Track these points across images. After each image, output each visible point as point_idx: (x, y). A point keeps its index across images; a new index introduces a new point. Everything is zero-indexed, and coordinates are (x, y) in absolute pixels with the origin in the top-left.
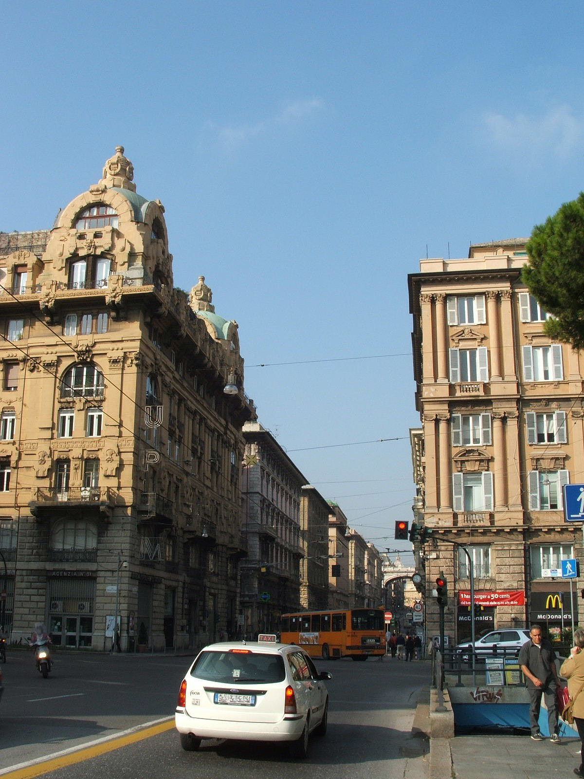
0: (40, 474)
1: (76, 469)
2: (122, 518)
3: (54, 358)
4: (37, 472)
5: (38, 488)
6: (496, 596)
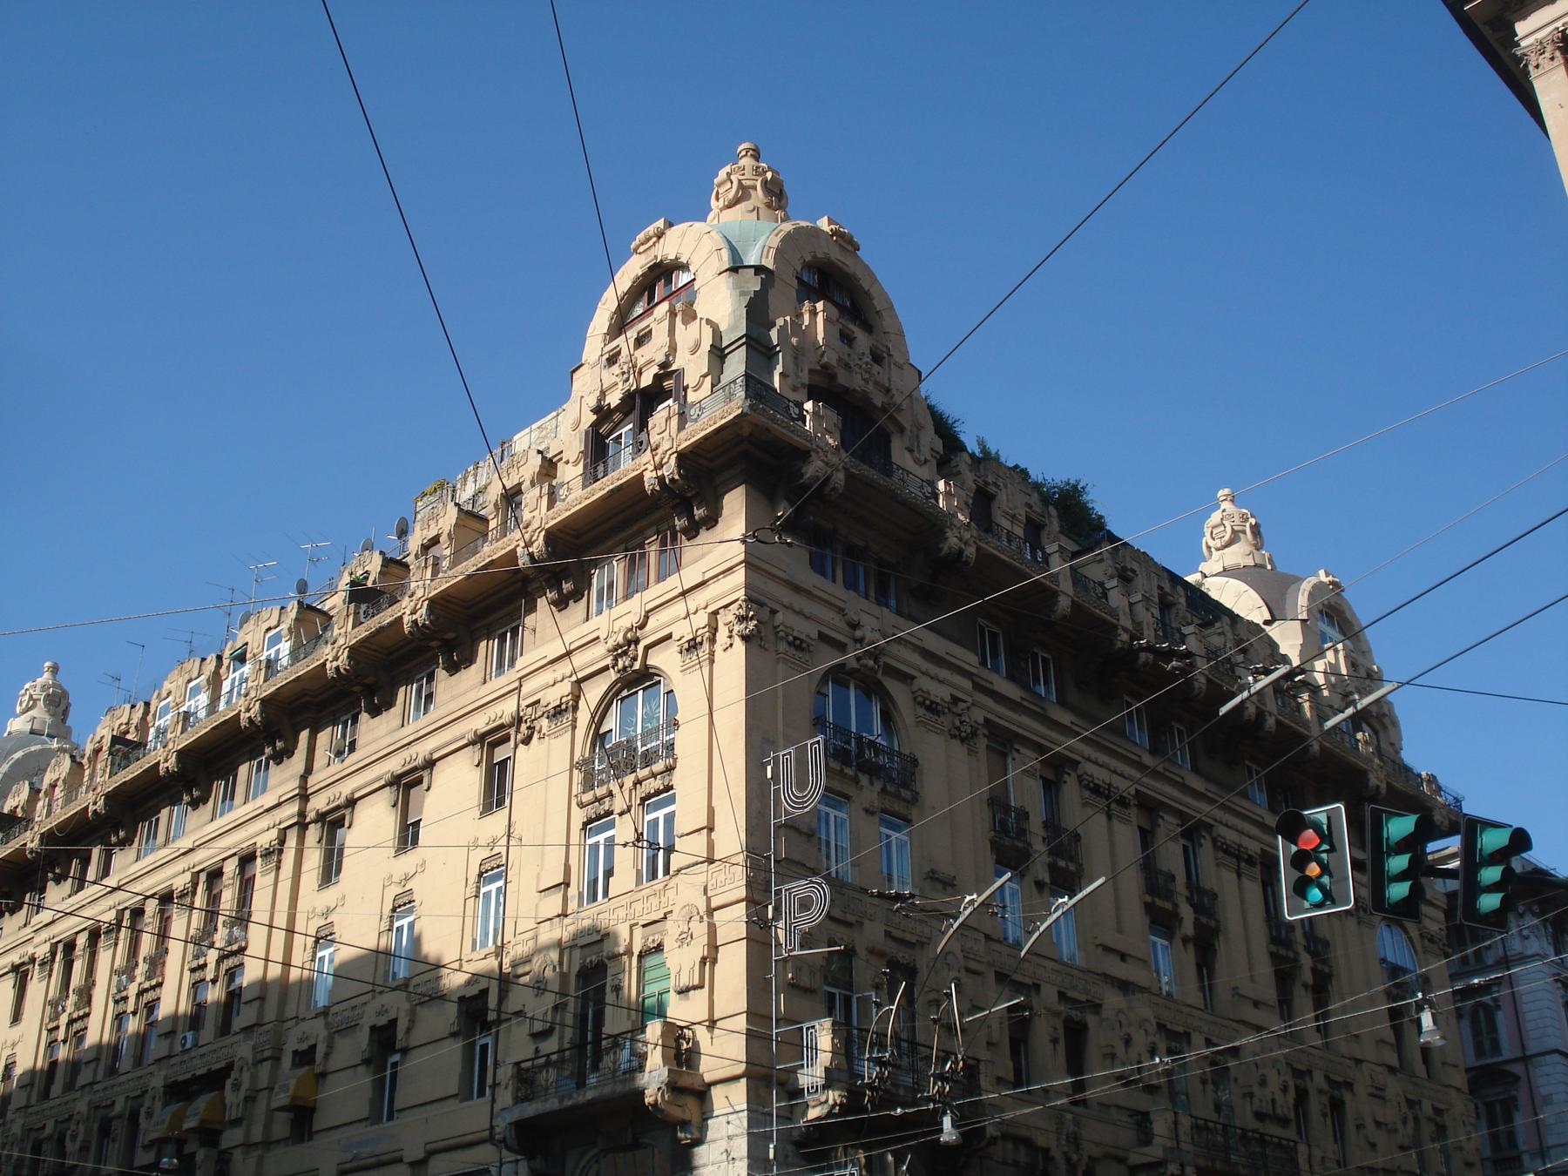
0: (538, 1027)
2: (723, 1119)
3: (566, 688)
5: (517, 1064)
6: (805, 905)
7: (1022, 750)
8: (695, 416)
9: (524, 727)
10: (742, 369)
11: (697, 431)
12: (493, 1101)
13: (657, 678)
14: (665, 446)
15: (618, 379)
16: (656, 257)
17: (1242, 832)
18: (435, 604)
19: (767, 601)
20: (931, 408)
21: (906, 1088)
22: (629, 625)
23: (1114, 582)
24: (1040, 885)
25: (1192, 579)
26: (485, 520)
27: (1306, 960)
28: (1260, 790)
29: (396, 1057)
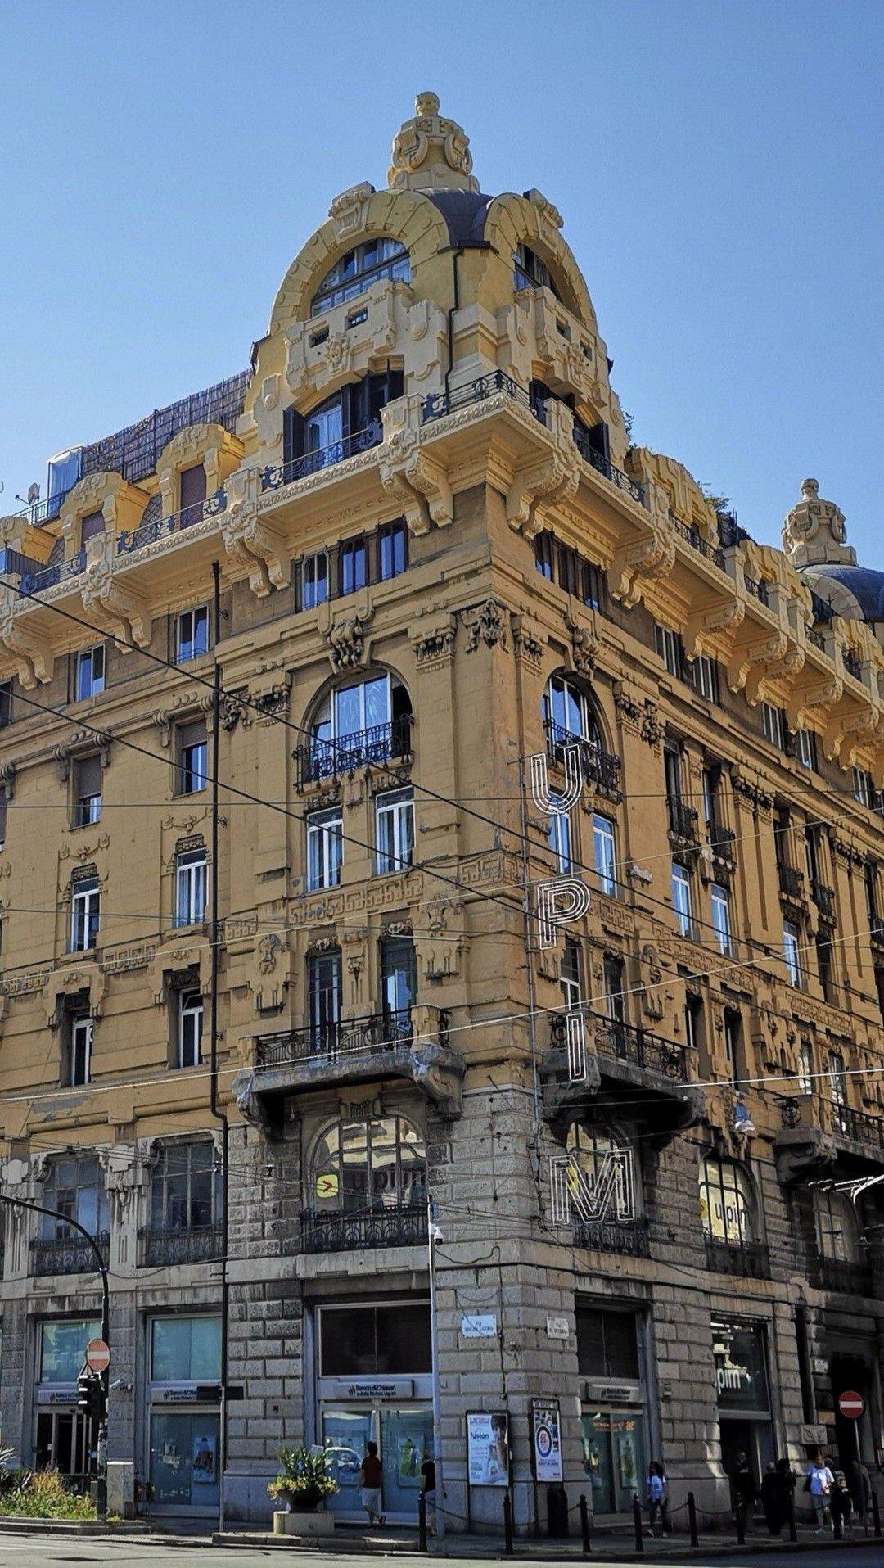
0: (267, 1002)
1: (356, 972)
2: (489, 1097)
4: (259, 998)
5: (257, 1037)
7: (691, 752)
19: (511, 607)
24: (705, 881)
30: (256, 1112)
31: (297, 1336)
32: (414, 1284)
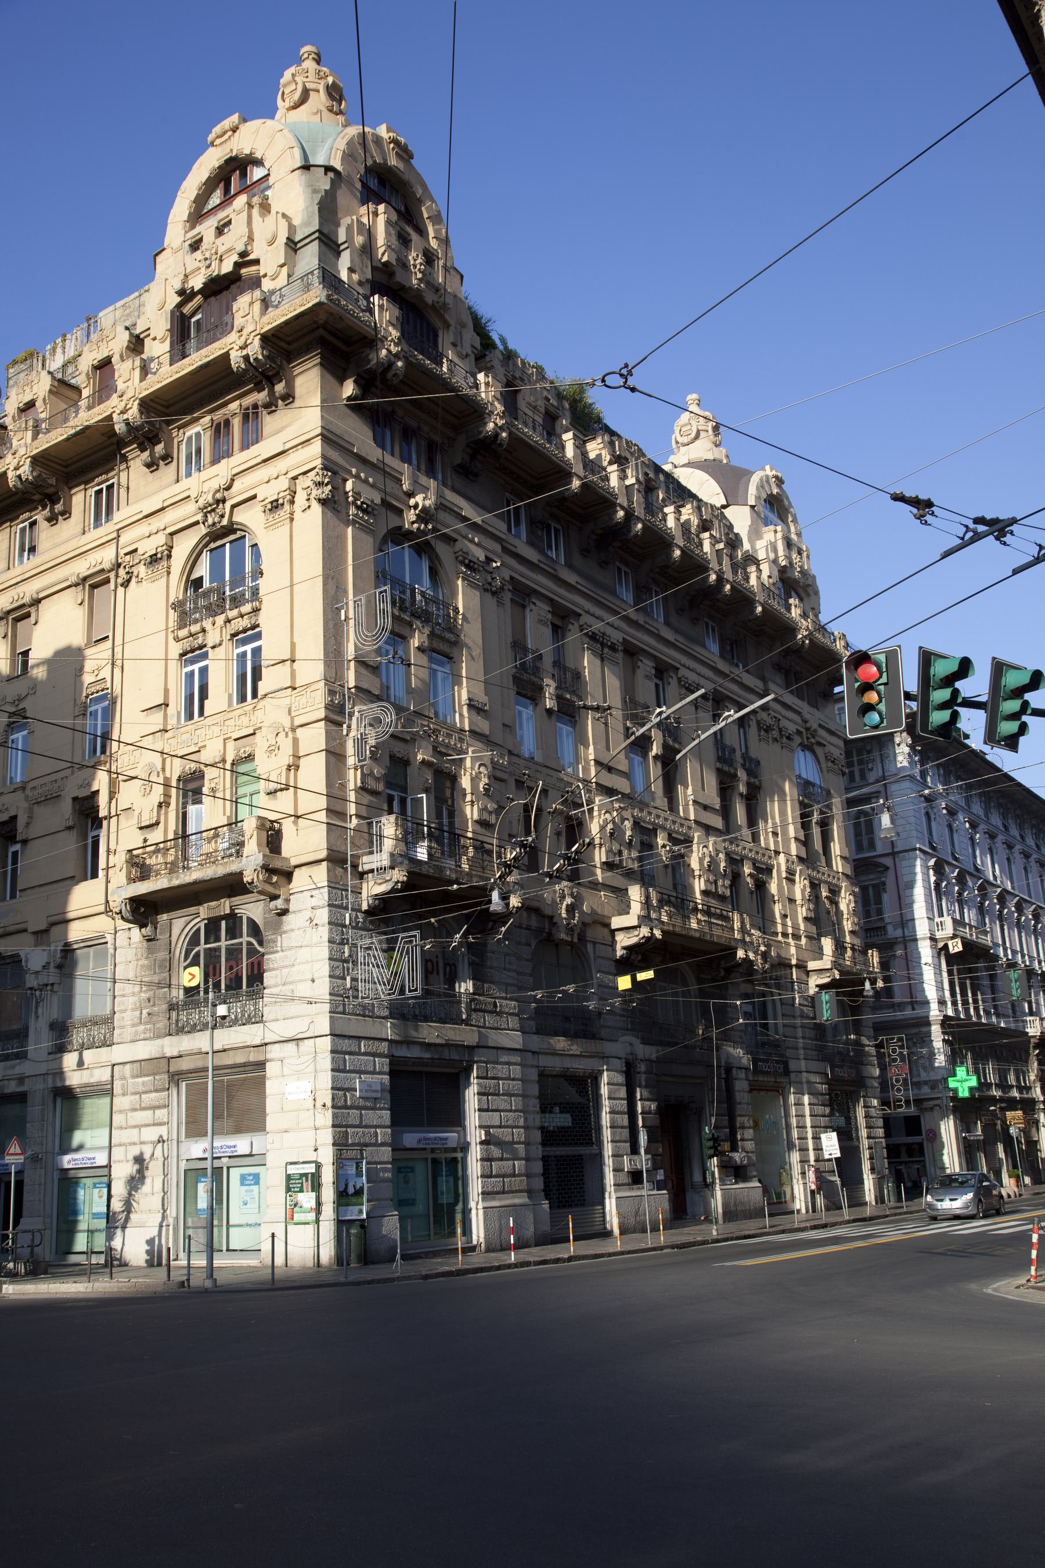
2: (309, 894)
3: (161, 539)
5: (130, 851)
7: (538, 603)
8: (276, 303)
9: (122, 572)
10: (315, 263)
11: (277, 317)
12: (108, 882)
13: (243, 533)
14: (249, 328)
15: (200, 265)
16: (232, 150)
17: (699, 674)
18: (37, 461)
20: (470, 308)
21: (450, 869)
22: (217, 487)
23: (615, 467)
24: (549, 712)
25: (667, 467)
26: (78, 390)
27: (742, 774)
28: (714, 642)
29: (17, 847)
30: (127, 914)
31: (164, 1106)
32: (254, 1057)
